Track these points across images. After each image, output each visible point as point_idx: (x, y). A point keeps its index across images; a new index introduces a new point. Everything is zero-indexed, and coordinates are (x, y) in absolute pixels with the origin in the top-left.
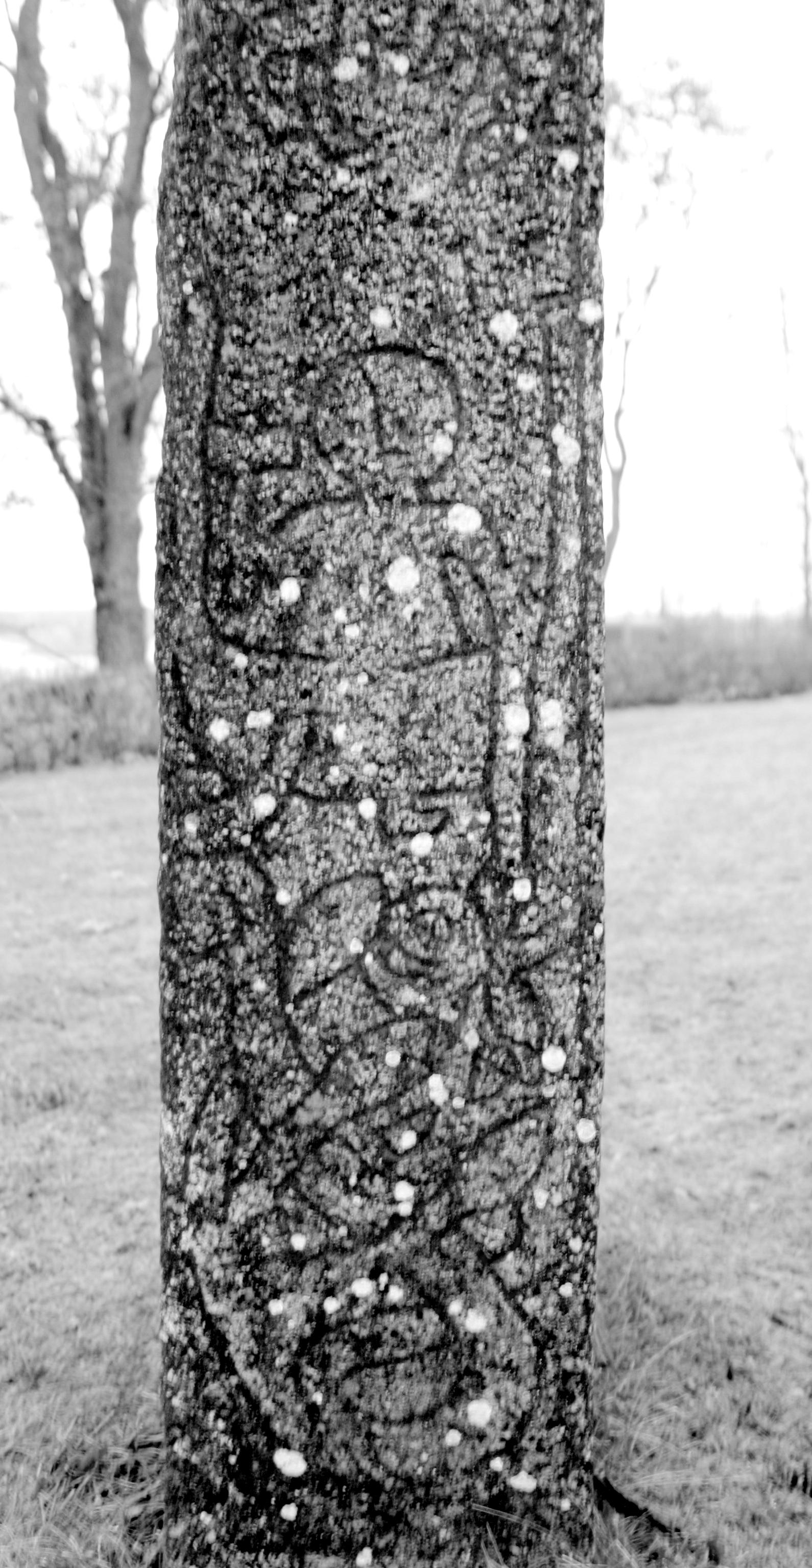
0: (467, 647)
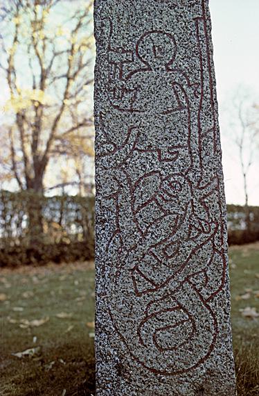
0: (181, 107)
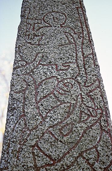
0: (70, 43)
